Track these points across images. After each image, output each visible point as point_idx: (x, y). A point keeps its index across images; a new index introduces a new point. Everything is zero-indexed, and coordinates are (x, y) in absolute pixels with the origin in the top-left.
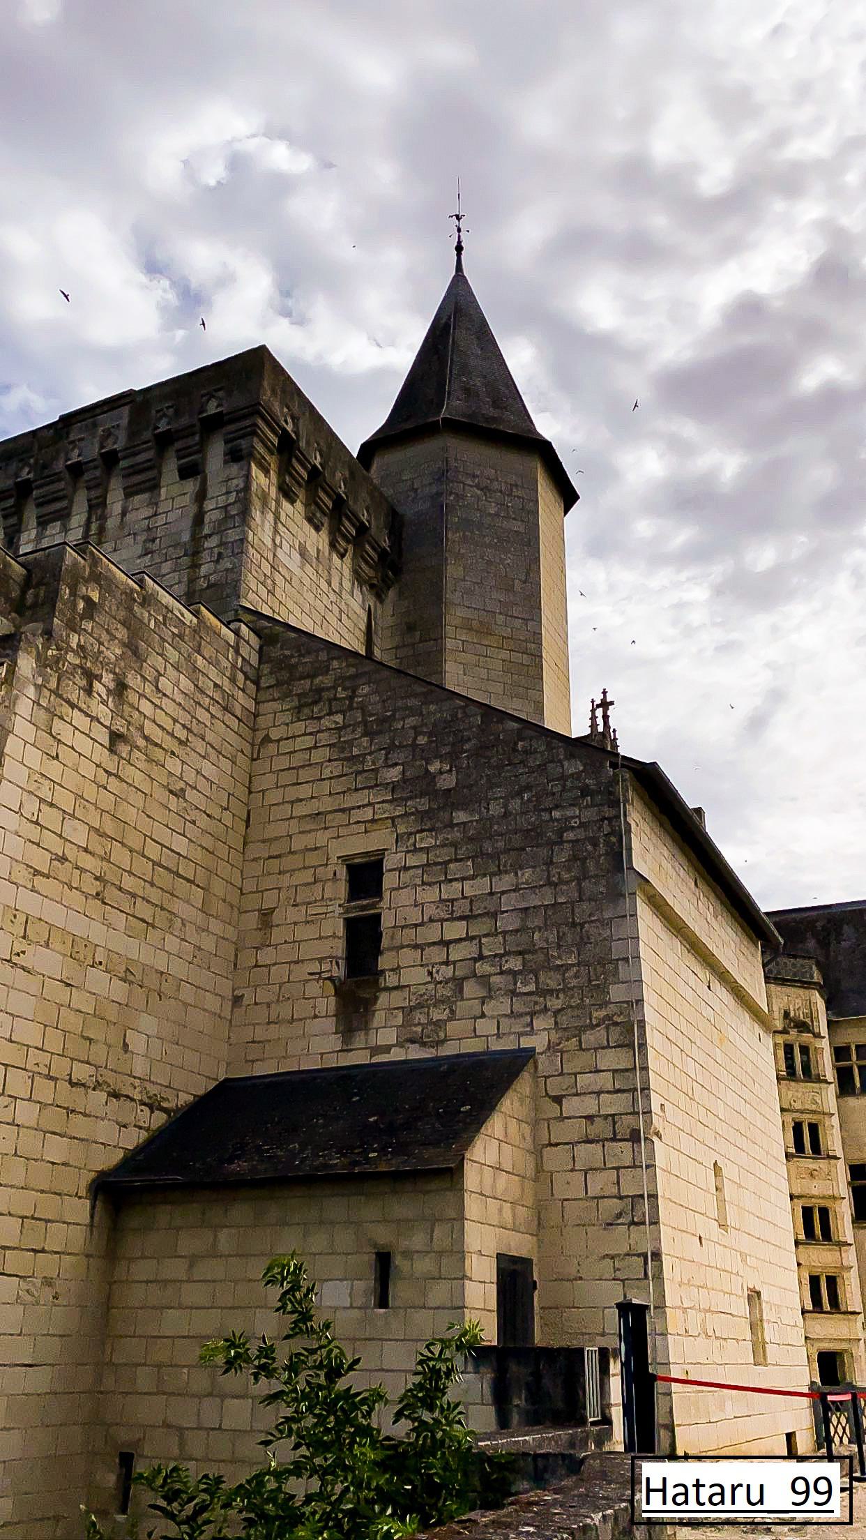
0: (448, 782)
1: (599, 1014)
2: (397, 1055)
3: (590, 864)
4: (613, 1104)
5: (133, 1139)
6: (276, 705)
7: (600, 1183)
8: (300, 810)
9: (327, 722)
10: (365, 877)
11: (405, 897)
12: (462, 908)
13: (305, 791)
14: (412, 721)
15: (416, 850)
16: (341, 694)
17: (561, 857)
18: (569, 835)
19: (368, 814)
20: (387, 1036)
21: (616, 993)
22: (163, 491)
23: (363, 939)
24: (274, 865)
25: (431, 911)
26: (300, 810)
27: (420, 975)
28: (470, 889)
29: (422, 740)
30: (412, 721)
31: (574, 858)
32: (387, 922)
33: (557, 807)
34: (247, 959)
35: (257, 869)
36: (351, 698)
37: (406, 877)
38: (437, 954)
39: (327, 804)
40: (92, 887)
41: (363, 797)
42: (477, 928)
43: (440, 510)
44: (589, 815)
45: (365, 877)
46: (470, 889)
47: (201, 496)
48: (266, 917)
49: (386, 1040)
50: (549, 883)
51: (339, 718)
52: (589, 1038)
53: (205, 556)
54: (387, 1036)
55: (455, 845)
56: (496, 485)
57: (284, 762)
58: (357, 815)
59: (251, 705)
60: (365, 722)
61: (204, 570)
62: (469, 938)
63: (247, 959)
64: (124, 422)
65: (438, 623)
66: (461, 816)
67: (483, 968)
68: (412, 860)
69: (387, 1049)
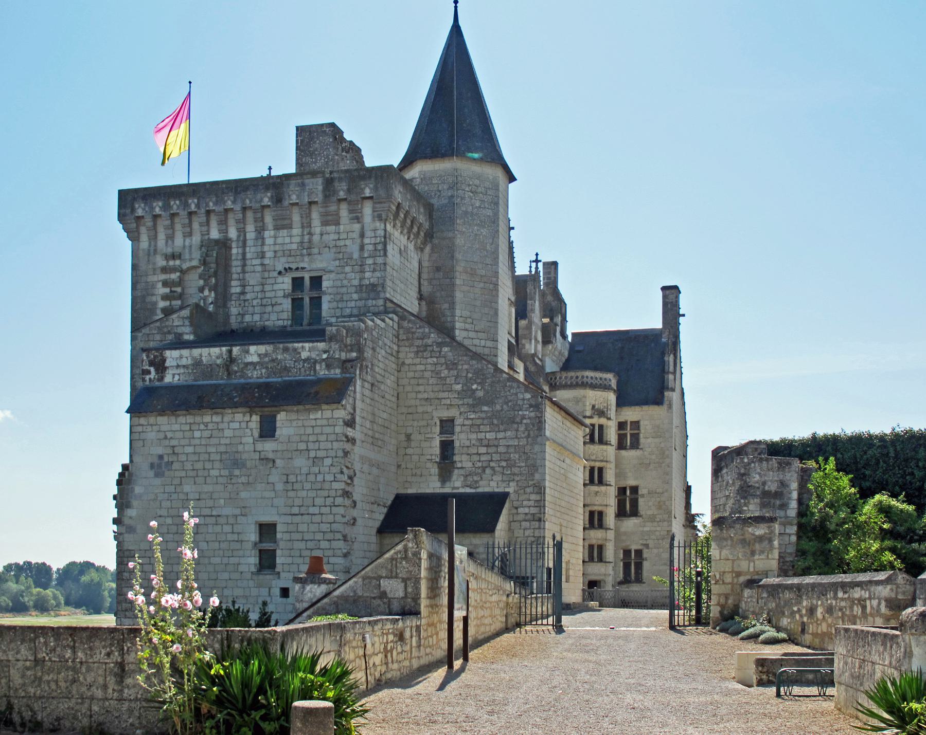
0: (480, 394)
1: (531, 483)
2: (462, 490)
3: (531, 433)
4: (533, 510)
5: (382, 517)
6: (407, 349)
7: (527, 533)
8: (420, 396)
9: (430, 361)
10: (447, 425)
11: (463, 436)
12: (485, 442)
13: (421, 388)
14: (466, 367)
15: (468, 419)
16: (435, 349)
17: (522, 428)
18: (525, 421)
19: (448, 402)
20: (458, 484)
21: (537, 476)
22: (342, 227)
23: (447, 448)
24: (410, 417)
25: (473, 442)
26: (420, 396)
27: (470, 464)
28: (489, 436)
29: (470, 375)
30: (466, 367)
31: (526, 429)
32: (457, 444)
33: (521, 410)
34: (402, 452)
35: (403, 417)
36: (440, 352)
37: (464, 428)
38: (476, 458)
39: (432, 395)
40: (370, 440)
41: (446, 395)
42: (491, 450)
43: (452, 203)
44: (532, 414)
45: (447, 425)
46: (489, 436)
47: (362, 235)
48: (408, 437)
49: (457, 485)
50: (516, 437)
51: (435, 360)
52: (528, 490)
53: (367, 268)
54: (458, 484)
55: (483, 419)
56: (480, 190)
57: (411, 374)
58: (444, 402)
59: (395, 348)
60: (446, 363)
61: (367, 275)
62: (487, 453)
63: (402, 452)
64: (320, 188)
65: (452, 269)
66: (485, 408)
67: (492, 464)
68: (467, 422)
69: (458, 488)
